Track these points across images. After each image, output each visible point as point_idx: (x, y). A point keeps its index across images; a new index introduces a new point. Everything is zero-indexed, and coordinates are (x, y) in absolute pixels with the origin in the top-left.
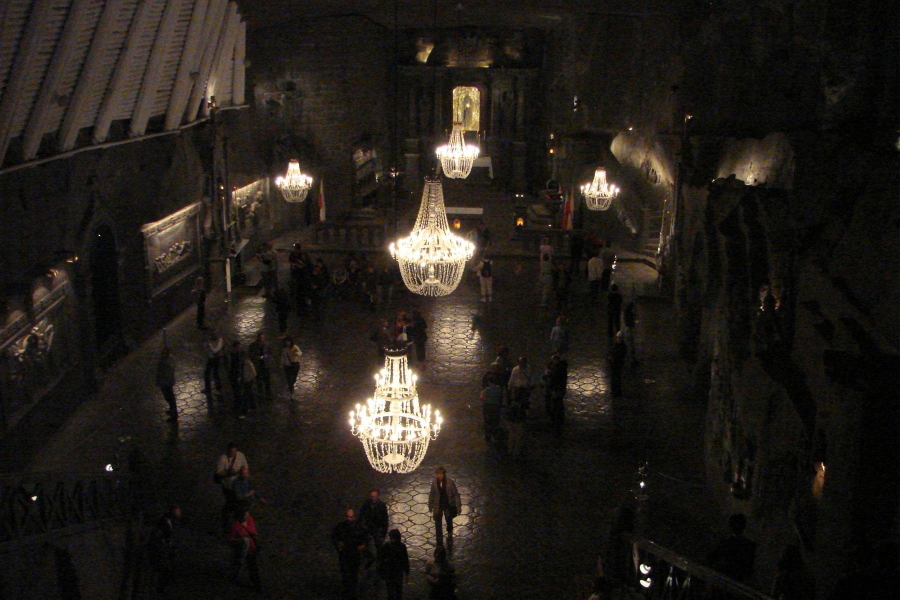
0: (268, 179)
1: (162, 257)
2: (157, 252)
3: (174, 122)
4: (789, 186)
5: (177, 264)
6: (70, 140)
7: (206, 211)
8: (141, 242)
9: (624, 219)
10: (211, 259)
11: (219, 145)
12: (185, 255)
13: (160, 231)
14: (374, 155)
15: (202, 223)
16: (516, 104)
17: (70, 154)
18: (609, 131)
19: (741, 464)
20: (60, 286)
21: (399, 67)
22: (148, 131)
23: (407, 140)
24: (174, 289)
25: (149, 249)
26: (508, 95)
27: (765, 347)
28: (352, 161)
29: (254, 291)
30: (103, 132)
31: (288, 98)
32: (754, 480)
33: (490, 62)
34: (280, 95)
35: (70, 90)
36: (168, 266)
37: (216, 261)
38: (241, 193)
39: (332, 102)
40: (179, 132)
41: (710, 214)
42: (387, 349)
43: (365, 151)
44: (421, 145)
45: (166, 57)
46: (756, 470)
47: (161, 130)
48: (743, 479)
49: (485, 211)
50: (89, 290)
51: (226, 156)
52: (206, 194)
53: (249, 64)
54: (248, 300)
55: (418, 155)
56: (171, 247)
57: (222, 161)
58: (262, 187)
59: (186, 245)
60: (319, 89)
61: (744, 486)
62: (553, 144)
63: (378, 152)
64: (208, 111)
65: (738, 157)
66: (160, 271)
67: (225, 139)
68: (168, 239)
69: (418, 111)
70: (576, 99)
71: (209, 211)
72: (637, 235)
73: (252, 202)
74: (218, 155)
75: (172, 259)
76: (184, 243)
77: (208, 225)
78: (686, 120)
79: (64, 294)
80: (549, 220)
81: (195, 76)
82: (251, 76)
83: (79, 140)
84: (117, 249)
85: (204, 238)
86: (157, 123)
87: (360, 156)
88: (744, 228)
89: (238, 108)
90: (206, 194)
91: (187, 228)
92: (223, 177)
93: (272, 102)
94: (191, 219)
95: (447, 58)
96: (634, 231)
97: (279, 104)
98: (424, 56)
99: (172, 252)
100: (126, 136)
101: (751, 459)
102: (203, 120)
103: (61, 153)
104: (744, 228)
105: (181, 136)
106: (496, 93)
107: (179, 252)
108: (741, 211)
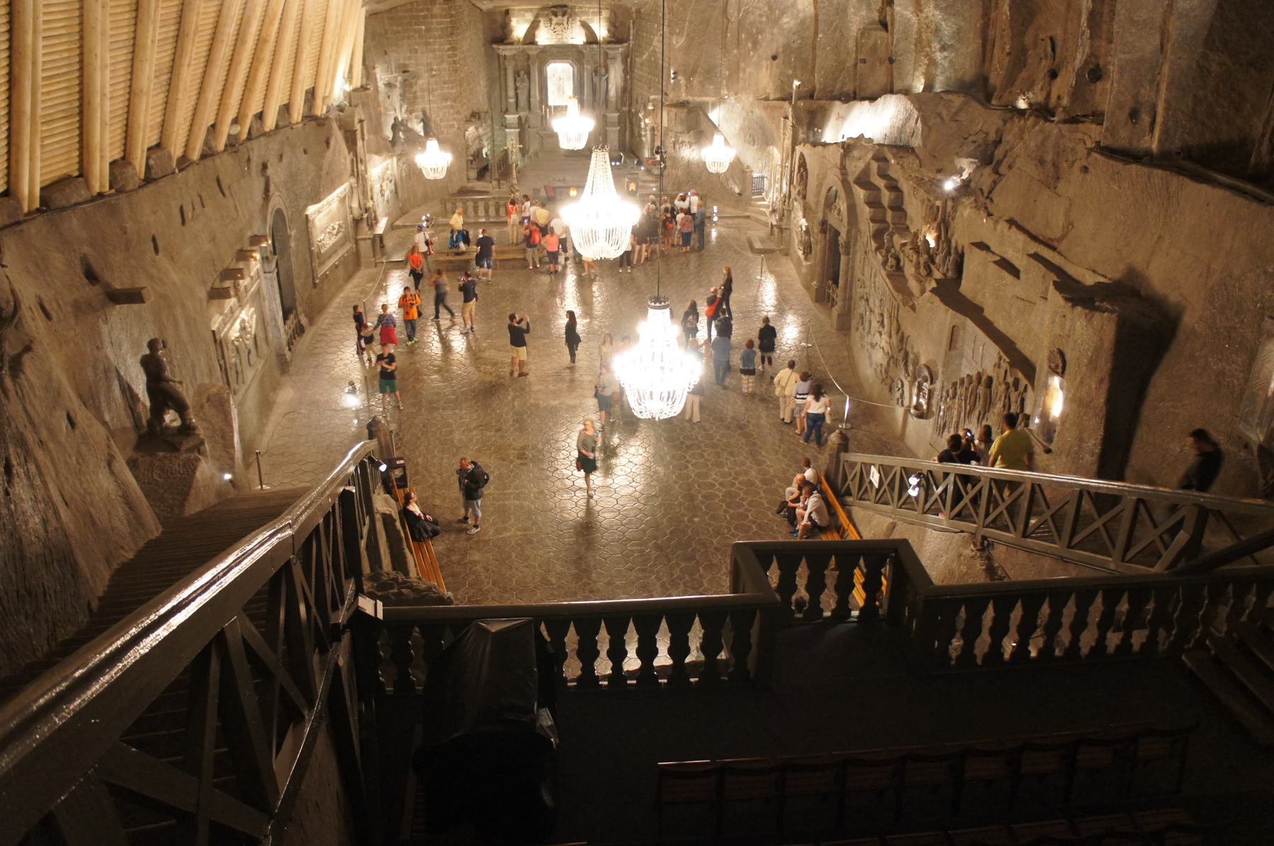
0: (395, 159)
1: (322, 237)
2: (318, 232)
4: (916, 142)
5: (334, 245)
7: (352, 193)
10: (358, 237)
11: (358, 127)
15: (350, 202)
16: (607, 80)
19: (920, 389)
20: (255, 270)
23: (506, 116)
25: (314, 230)
27: (934, 285)
31: (405, 80)
32: (934, 402)
34: (396, 77)
36: (328, 246)
37: (365, 239)
39: (445, 83)
41: (843, 168)
42: (653, 304)
43: (477, 128)
44: (520, 118)
46: (937, 394)
48: (923, 401)
51: (363, 139)
52: (352, 174)
55: (518, 130)
56: (327, 228)
58: (390, 166)
59: (340, 226)
61: (925, 407)
62: (647, 114)
65: (842, 118)
66: (322, 251)
67: (361, 121)
68: (325, 220)
69: (516, 89)
71: (355, 191)
72: (740, 194)
73: (383, 181)
75: (330, 239)
76: (337, 223)
77: (355, 205)
78: (794, 87)
79: (259, 277)
80: (652, 185)
85: (354, 219)
87: (471, 130)
88: (880, 183)
90: (352, 174)
92: (362, 157)
93: (389, 85)
94: (342, 200)
96: (737, 190)
97: (396, 86)
99: (329, 233)
101: (932, 383)
104: (880, 183)
107: (335, 232)
108: (874, 165)
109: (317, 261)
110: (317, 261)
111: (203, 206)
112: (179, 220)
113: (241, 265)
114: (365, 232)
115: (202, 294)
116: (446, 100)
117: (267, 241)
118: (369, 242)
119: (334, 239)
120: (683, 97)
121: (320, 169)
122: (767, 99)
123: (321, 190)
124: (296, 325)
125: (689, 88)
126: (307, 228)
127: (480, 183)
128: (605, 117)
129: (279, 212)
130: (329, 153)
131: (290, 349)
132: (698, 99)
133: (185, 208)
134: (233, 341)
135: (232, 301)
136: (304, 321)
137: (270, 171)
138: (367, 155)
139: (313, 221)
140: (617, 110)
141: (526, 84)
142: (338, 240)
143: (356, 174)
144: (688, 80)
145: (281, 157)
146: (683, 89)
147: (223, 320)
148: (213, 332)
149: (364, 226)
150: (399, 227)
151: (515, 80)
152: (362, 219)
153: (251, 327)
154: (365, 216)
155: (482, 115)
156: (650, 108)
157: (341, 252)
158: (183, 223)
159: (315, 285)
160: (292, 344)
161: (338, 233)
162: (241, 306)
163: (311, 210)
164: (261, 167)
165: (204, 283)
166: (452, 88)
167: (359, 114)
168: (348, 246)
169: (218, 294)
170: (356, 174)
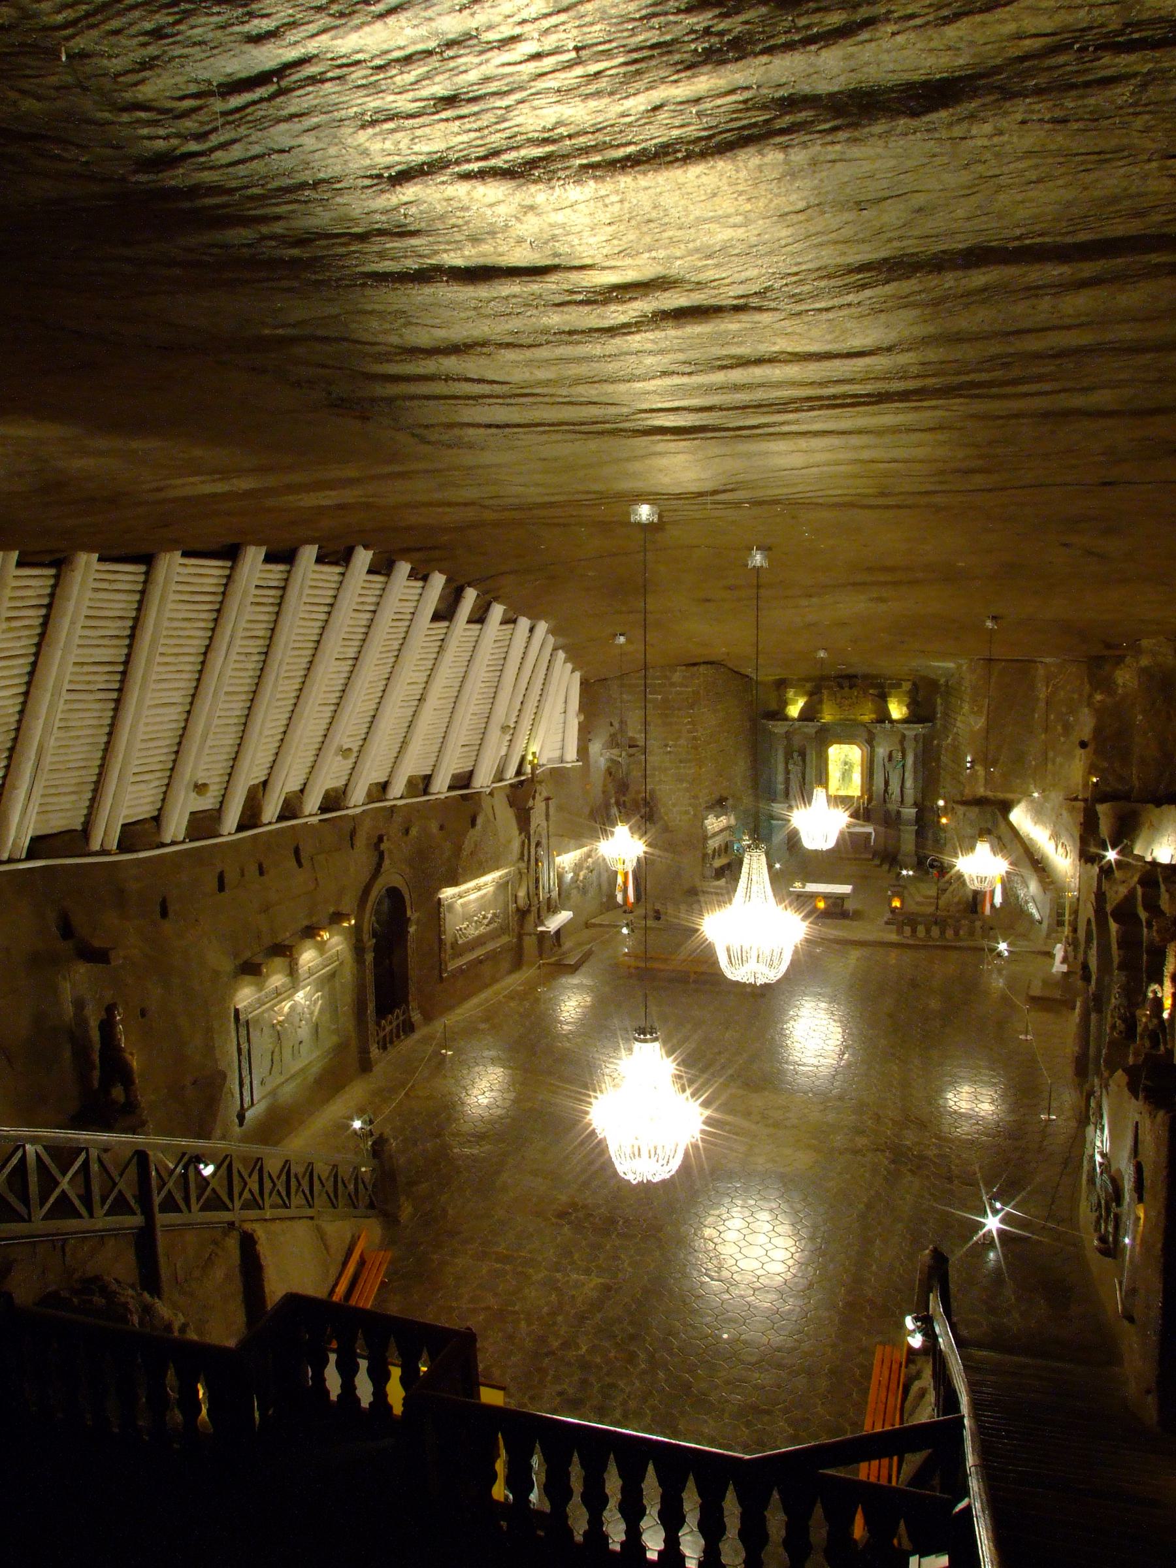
3: (483, 780)
6: (358, 796)
8: (436, 910)
9: (1027, 902)
12: (492, 926)
13: (461, 897)
14: (733, 821)
16: (903, 766)
17: (358, 810)
18: (1009, 796)
21: (764, 721)
22: (451, 788)
24: (479, 962)
26: (894, 754)
28: (702, 826)
29: (574, 969)
30: (398, 788)
33: (873, 716)
35: (361, 743)
38: (567, 860)
39: (681, 762)
40: (488, 790)
45: (472, 709)
47: (467, 786)
49: (854, 890)
50: (369, 957)
53: (582, 718)
54: (563, 980)
57: (544, 824)
59: (494, 914)
60: (666, 746)
63: (737, 819)
64: (528, 769)
68: (472, 907)
69: (787, 772)
70: (969, 759)
73: (581, 870)
74: (537, 818)
75: (476, 929)
77: (522, 893)
81: (511, 730)
82: (585, 733)
83: (369, 794)
84: (409, 913)
85: (518, 909)
86: (463, 781)
87: (714, 823)
89: (569, 765)
90: (521, 858)
91: (495, 894)
92: (544, 841)
94: (502, 886)
95: (820, 711)
98: (794, 711)
100: (426, 792)
102: (523, 778)
103: (348, 808)
105: (491, 794)
106: (881, 751)
107: (486, 921)
109: (449, 951)
110: (449, 951)
111: (261, 873)
112: (215, 884)
113: (309, 943)
114: (529, 927)
115: (227, 965)
116: (681, 781)
117: (349, 920)
118: (534, 938)
119: (482, 930)
120: (981, 791)
121: (458, 849)
122: (1076, 799)
123: (460, 870)
124: (404, 1021)
125: (987, 782)
126: (439, 913)
127: (717, 883)
128: (899, 812)
129: (394, 894)
130: (474, 834)
131: (385, 1048)
132: (1000, 796)
133: (226, 875)
134: (273, 1026)
135: (277, 980)
136: (416, 1017)
137: (383, 846)
138: (552, 840)
139: (451, 907)
140: (916, 804)
141: (799, 769)
142: (491, 932)
143: (526, 858)
144: (986, 769)
145: (407, 831)
146: (981, 781)
147: (259, 999)
148: (237, 1011)
149: (532, 917)
150: (594, 925)
151: (787, 764)
152: (529, 911)
153: (312, 1013)
154: (534, 909)
155: (730, 802)
156: (941, 803)
157: (490, 946)
158: (221, 887)
159: (441, 979)
160: (391, 1042)
161: (490, 923)
162: (295, 986)
163: (447, 893)
164: (375, 840)
165: (236, 956)
166: (690, 768)
167: (543, 791)
168: (505, 939)
169: (251, 970)
170: (526, 858)
